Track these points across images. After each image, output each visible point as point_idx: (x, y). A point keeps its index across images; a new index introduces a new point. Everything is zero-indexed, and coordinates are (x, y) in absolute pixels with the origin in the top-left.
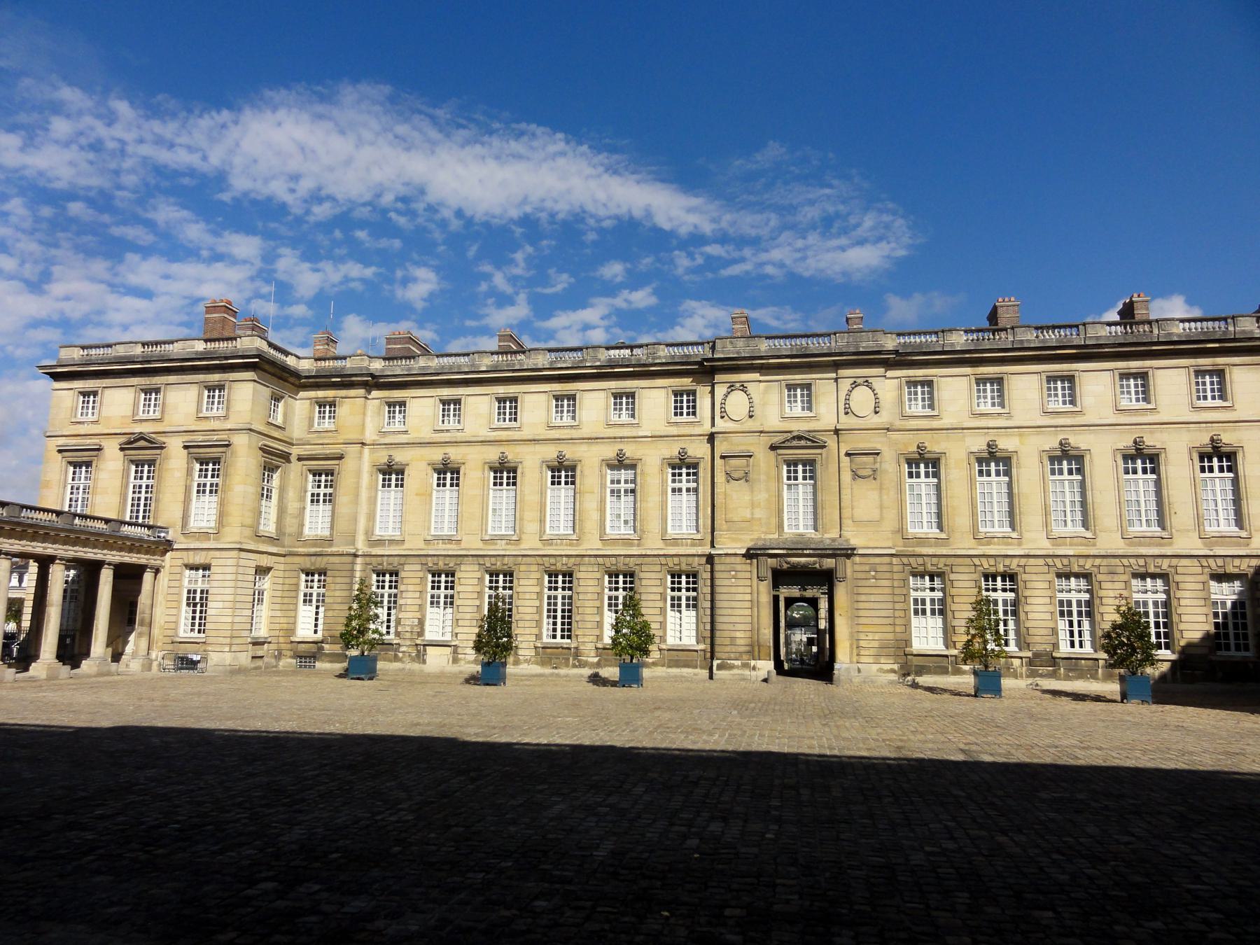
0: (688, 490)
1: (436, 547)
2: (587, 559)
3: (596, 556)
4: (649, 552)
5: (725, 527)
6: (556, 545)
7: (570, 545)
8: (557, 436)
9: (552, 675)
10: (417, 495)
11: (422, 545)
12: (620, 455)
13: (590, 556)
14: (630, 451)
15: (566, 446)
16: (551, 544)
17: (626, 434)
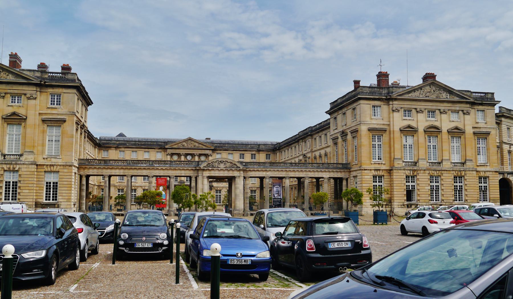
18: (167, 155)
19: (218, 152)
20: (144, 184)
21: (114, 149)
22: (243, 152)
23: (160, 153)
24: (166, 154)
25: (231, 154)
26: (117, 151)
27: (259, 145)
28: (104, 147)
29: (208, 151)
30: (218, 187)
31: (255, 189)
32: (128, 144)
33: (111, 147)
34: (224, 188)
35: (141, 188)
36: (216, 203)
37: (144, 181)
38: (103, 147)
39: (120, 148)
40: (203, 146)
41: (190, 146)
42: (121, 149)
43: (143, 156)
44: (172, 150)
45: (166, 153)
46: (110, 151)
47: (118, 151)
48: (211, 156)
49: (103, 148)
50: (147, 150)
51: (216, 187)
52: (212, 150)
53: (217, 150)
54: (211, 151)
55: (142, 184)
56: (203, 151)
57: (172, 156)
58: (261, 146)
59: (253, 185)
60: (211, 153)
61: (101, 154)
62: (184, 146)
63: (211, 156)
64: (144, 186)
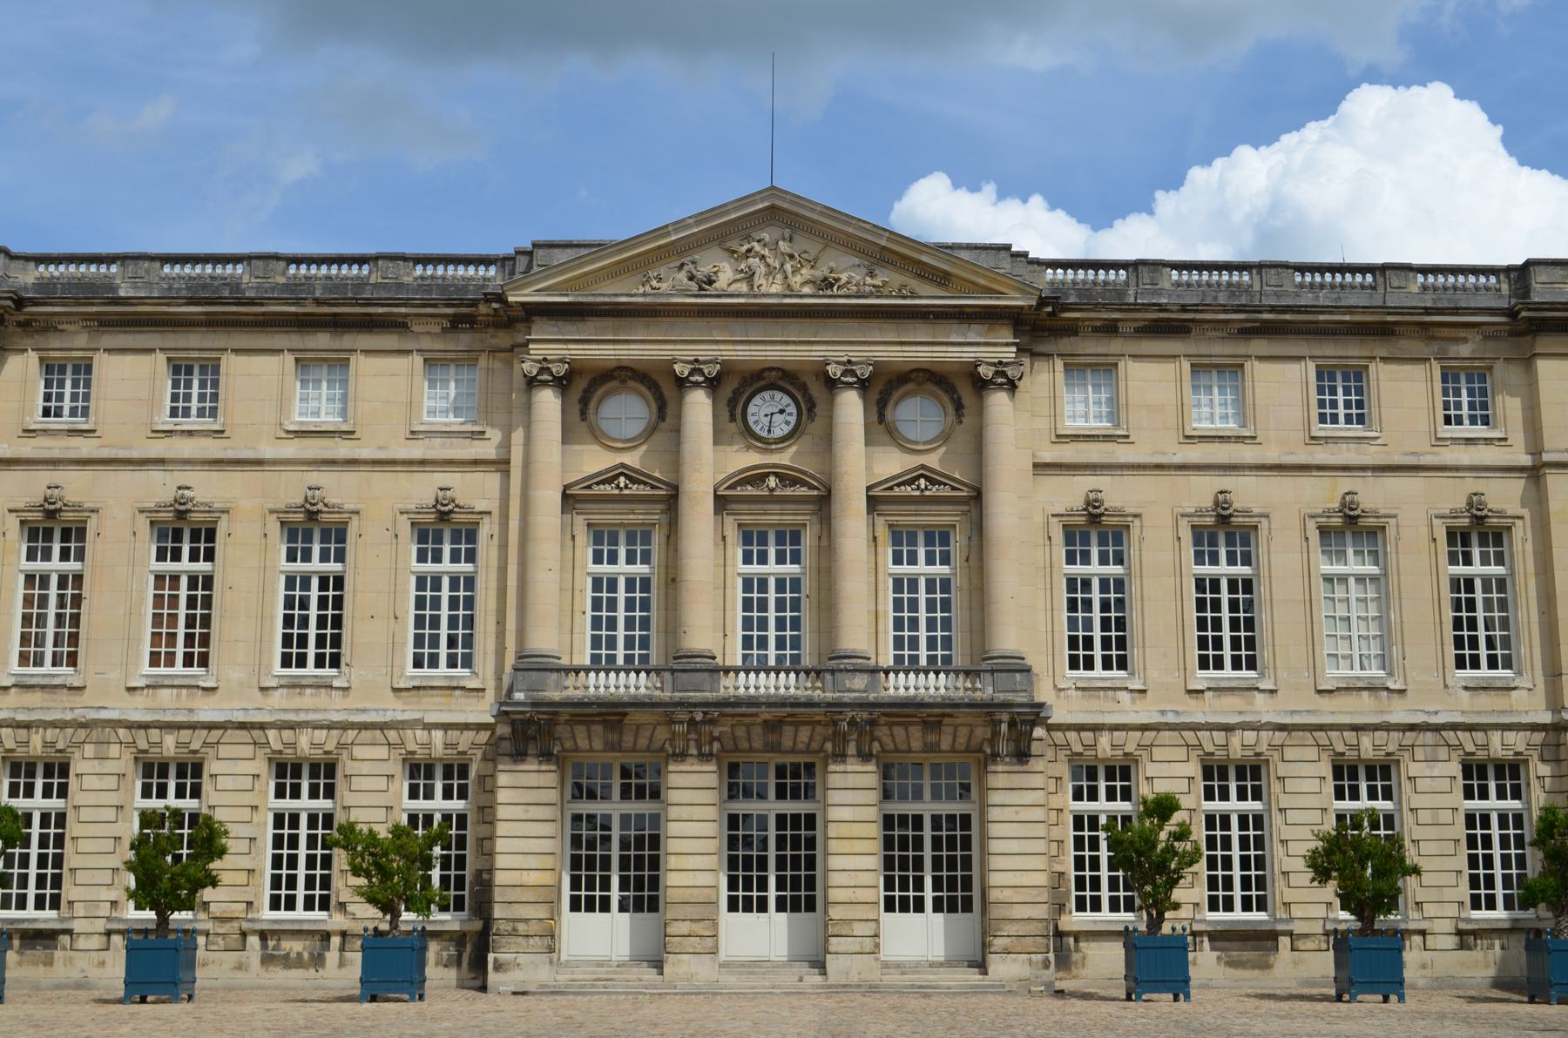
18: (532, 383)
19: (1090, 346)
20: (278, 699)
22: (1352, 350)
23: (465, 374)
24: (519, 381)
25: (1221, 368)
27: (1521, 274)
29: (974, 333)
30: (1096, 728)
31: (1517, 740)
34: (1166, 736)
35: (248, 751)
36: (1081, 906)
37: (294, 671)
39: (49, 326)
40: (915, 284)
41: (775, 289)
43: (283, 405)
44: (589, 328)
45: (516, 367)
48: (1012, 386)
50: (322, 340)
51: (1080, 728)
52: (1014, 318)
53: (1072, 330)
54: (1006, 335)
56: (921, 332)
57: (584, 402)
58: (1539, 278)
59: (1485, 701)
60: (1009, 354)
63: (1012, 386)
64: (282, 726)
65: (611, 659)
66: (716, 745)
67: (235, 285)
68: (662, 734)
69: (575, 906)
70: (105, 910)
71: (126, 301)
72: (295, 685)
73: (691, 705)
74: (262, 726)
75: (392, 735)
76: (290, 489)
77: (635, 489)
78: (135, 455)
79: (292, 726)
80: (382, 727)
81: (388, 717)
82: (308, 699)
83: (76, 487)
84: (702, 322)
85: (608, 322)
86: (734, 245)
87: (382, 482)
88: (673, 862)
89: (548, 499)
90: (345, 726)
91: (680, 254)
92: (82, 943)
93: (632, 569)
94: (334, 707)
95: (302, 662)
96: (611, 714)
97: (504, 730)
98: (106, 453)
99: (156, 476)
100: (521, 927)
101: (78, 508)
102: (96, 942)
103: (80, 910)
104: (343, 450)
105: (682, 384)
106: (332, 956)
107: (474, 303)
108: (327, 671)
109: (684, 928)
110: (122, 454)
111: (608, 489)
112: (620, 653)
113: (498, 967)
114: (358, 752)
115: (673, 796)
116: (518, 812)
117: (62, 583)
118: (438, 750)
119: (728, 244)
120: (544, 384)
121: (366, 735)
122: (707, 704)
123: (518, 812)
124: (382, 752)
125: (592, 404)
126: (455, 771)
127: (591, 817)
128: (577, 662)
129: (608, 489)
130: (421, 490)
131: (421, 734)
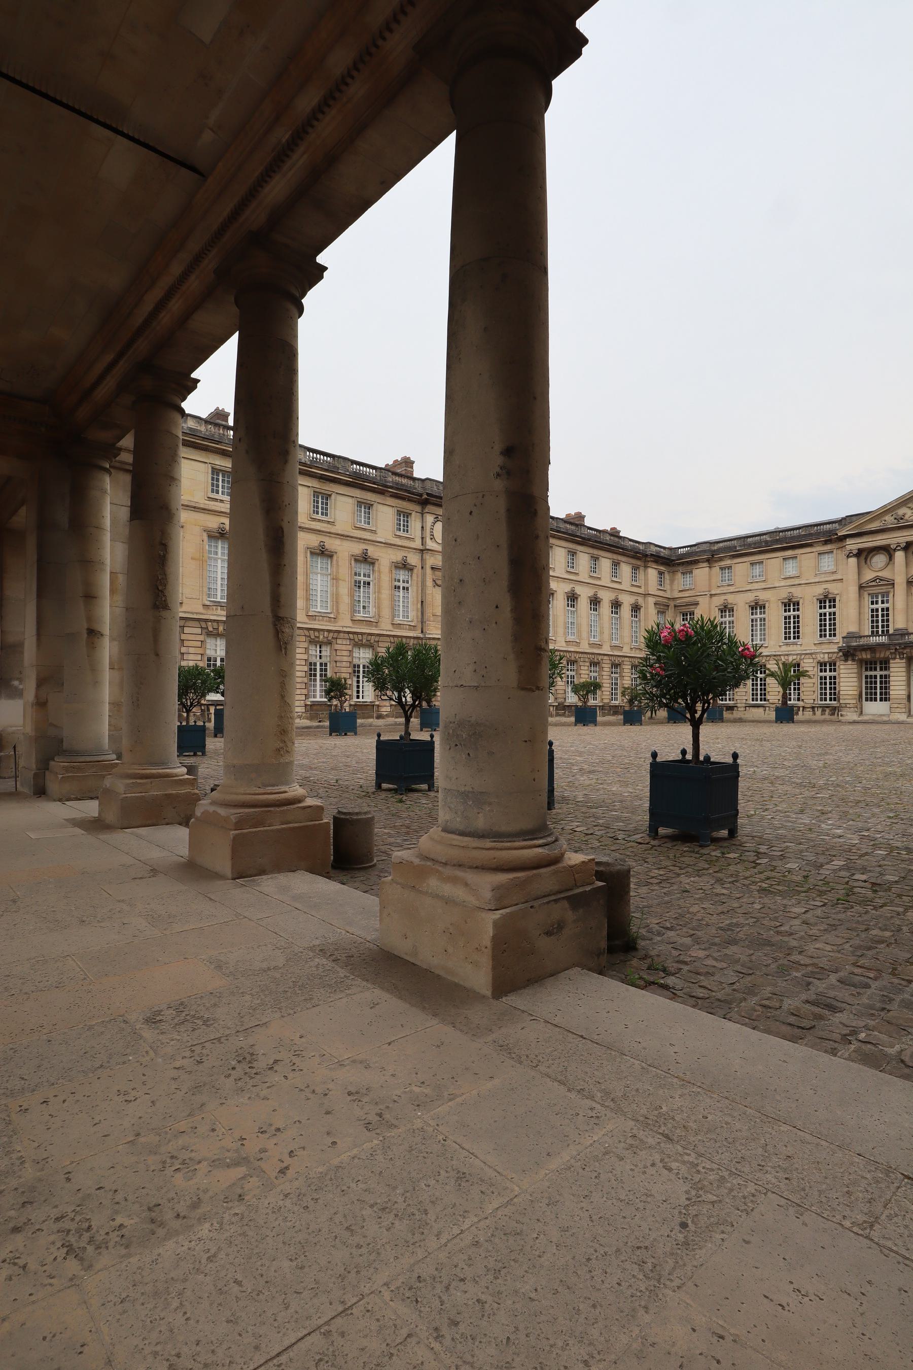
0: (404, 588)
1: (215, 613)
2: (342, 635)
3: (349, 633)
4: (385, 633)
5: (432, 619)
6: (319, 620)
7: (330, 621)
8: (318, 528)
9: (318, 727)
10: (192, 558)
11: (200, 609)
12: (365, 552)
13: (345, 632)
14: (373, 552)
15: (328, 538)
16: (315, 620)
17: (369, 538)
18: (848, 557)
20: (784, 648)
21: (706, 564)
23: (830, 555)
26: (714, 569)
28: (683, 564)
32: (740, 546)
33: (696, 562)
37: (788, 641)
38: (679, 564)
39: (721, 559)
42: (723, 563)
46: (696, 572)
47: (716, 570)
49: (681, 569)
55: (778, 649)
57: (866, 559)
61: (676, 582)
62: (900, 519)
64: (785, 655)
65: (877, 632)
66: (905, 655)
67: (766, 542)
68: (888, 653)
69: (867, 700)
70: (744, 701)
71: (738, 551)
72: (787, 644)
73: (896, 644)
74: (780, 655)
75: (814, 656)
76: (784, 594)
77: (882, 583)
78: (744, 589)
79: (787, 655)
80: (811, 654)
81: (813, 651)
82: (791, 648)
83: (731, 599)
84: (900, 531)
85: (870, 535)
86: (909, 505)
87: (808, 588)
88: (892, 688)
89: (853, 589)
90: (801, 655)
91: (892, 512)
92: (739, 709)
93: (883, 605)
94: (797, 649)
95: (790, 638)
96: (872, 648)
97: (841, 654)
98: (737, 590)
99: (749, 594)
100: (848, 705)
101: (732, 604)
102: (743, 709)
103: (739, 701)
104: (797, 581)
105: (895, 550)
106: (800, 713)
107: (830, 536)
108: (796, 640)
109: (896, 706)
110: (741, 590)
111: (874, 583)
112: (880, 629)
113: (842, 715)
114: (805, 661)
115: (891, 670)
116: (846, 675)
117: (729, 623)
118: (826, 660)
119: (909, 505)
120: (851, 557)
121: (807, 656)
122: (900, 644)
123: (846, 675)
124: (811, 661)
125: (869, 559)
126: (833, 664)
127: (871, 676)
128: (866, 634)
129: (874, 583)
130: (819, 590)
131: (822, 656)
